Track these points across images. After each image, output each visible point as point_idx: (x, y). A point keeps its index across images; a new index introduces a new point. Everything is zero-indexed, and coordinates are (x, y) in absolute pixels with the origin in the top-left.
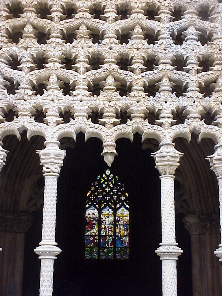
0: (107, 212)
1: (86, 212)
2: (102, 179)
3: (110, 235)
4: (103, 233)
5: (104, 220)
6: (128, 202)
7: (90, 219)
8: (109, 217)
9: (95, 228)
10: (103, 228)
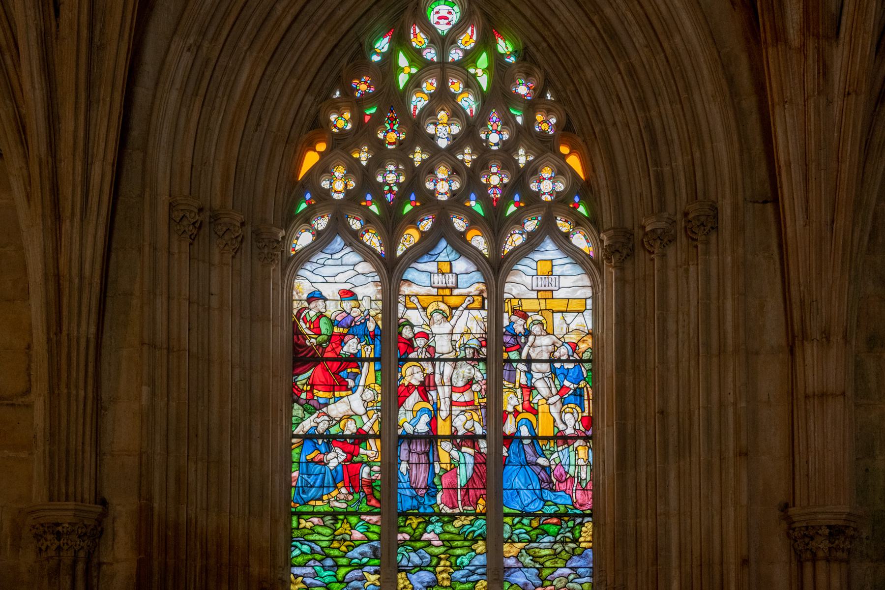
0: (438, 280)
2: (402, 60)
4: (412, 417)
5: (417, 330)
6: (582, 209)
7: (324, 326)
9: (360, 389)
10: (410, 388)
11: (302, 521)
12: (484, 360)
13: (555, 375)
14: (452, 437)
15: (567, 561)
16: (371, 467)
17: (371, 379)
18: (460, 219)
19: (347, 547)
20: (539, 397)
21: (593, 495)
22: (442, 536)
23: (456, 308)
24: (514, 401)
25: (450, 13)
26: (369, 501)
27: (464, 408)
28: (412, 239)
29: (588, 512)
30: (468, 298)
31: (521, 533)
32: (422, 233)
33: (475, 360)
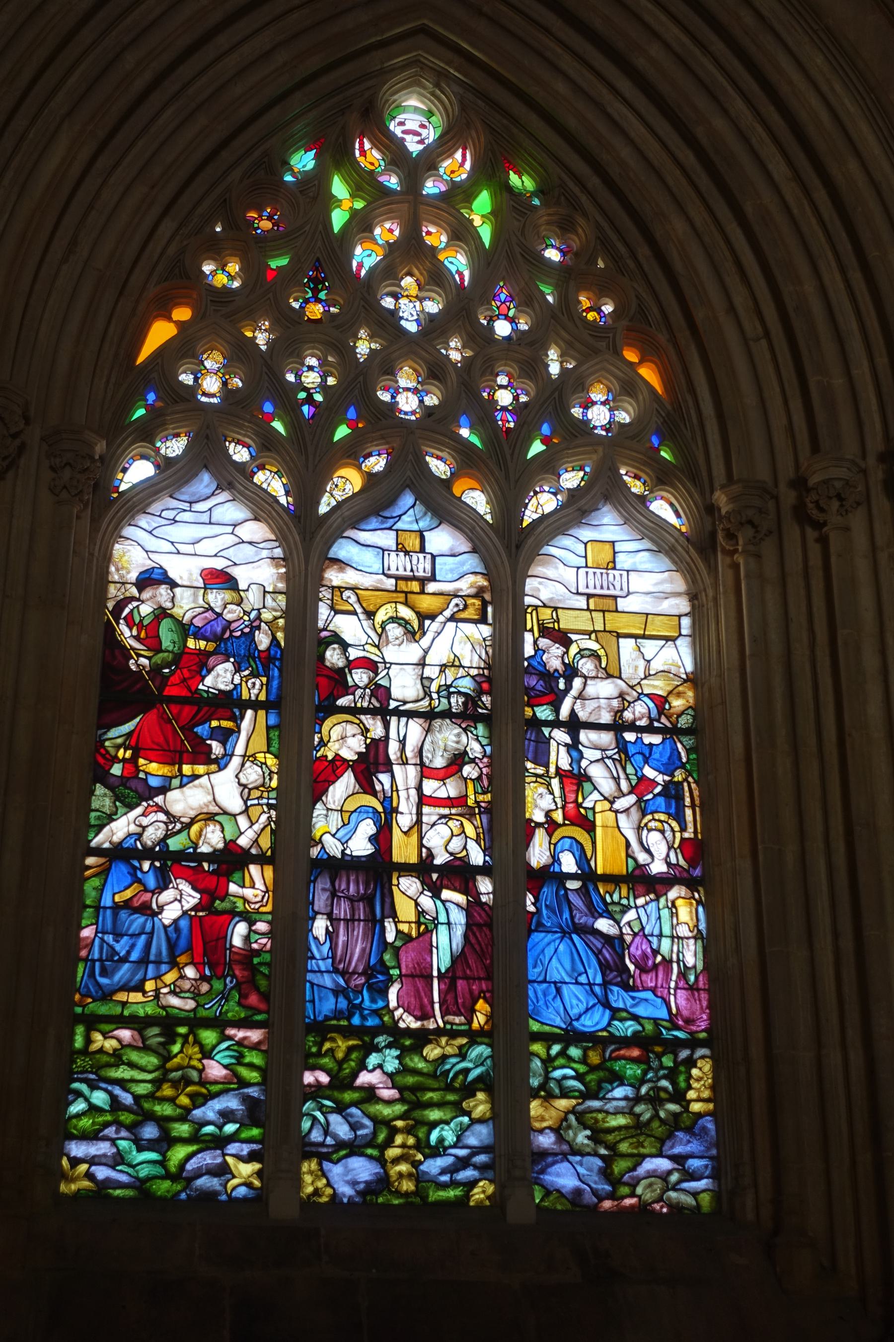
0: (398, 563)
2: (339, 188)
3: (441, 859)
4: (340, 826)
5: (353, 654)
7: (167, 636)
8: (432, 627)
9: (236, 761)
10: (338, 766)
11: (97, 1037)
12: (487, 720)
14: (423, 868)
15: (662, 1141)
16: (251, 923)
17: (259, 741)
18: (439, 458)
19: (191, 1096)
20: (595, 796)
21: (709, 1001)
22: (398, 1078)
23: (433, 617)
24: (546, 802)
25: (423, 126)
26: (243, 996)
27: (446, 811)
28: (348, 486)
29: (703, 1035)
30: (455, 601)
31: (565, 1077)
32: (371, 478)
33: (468, 716)
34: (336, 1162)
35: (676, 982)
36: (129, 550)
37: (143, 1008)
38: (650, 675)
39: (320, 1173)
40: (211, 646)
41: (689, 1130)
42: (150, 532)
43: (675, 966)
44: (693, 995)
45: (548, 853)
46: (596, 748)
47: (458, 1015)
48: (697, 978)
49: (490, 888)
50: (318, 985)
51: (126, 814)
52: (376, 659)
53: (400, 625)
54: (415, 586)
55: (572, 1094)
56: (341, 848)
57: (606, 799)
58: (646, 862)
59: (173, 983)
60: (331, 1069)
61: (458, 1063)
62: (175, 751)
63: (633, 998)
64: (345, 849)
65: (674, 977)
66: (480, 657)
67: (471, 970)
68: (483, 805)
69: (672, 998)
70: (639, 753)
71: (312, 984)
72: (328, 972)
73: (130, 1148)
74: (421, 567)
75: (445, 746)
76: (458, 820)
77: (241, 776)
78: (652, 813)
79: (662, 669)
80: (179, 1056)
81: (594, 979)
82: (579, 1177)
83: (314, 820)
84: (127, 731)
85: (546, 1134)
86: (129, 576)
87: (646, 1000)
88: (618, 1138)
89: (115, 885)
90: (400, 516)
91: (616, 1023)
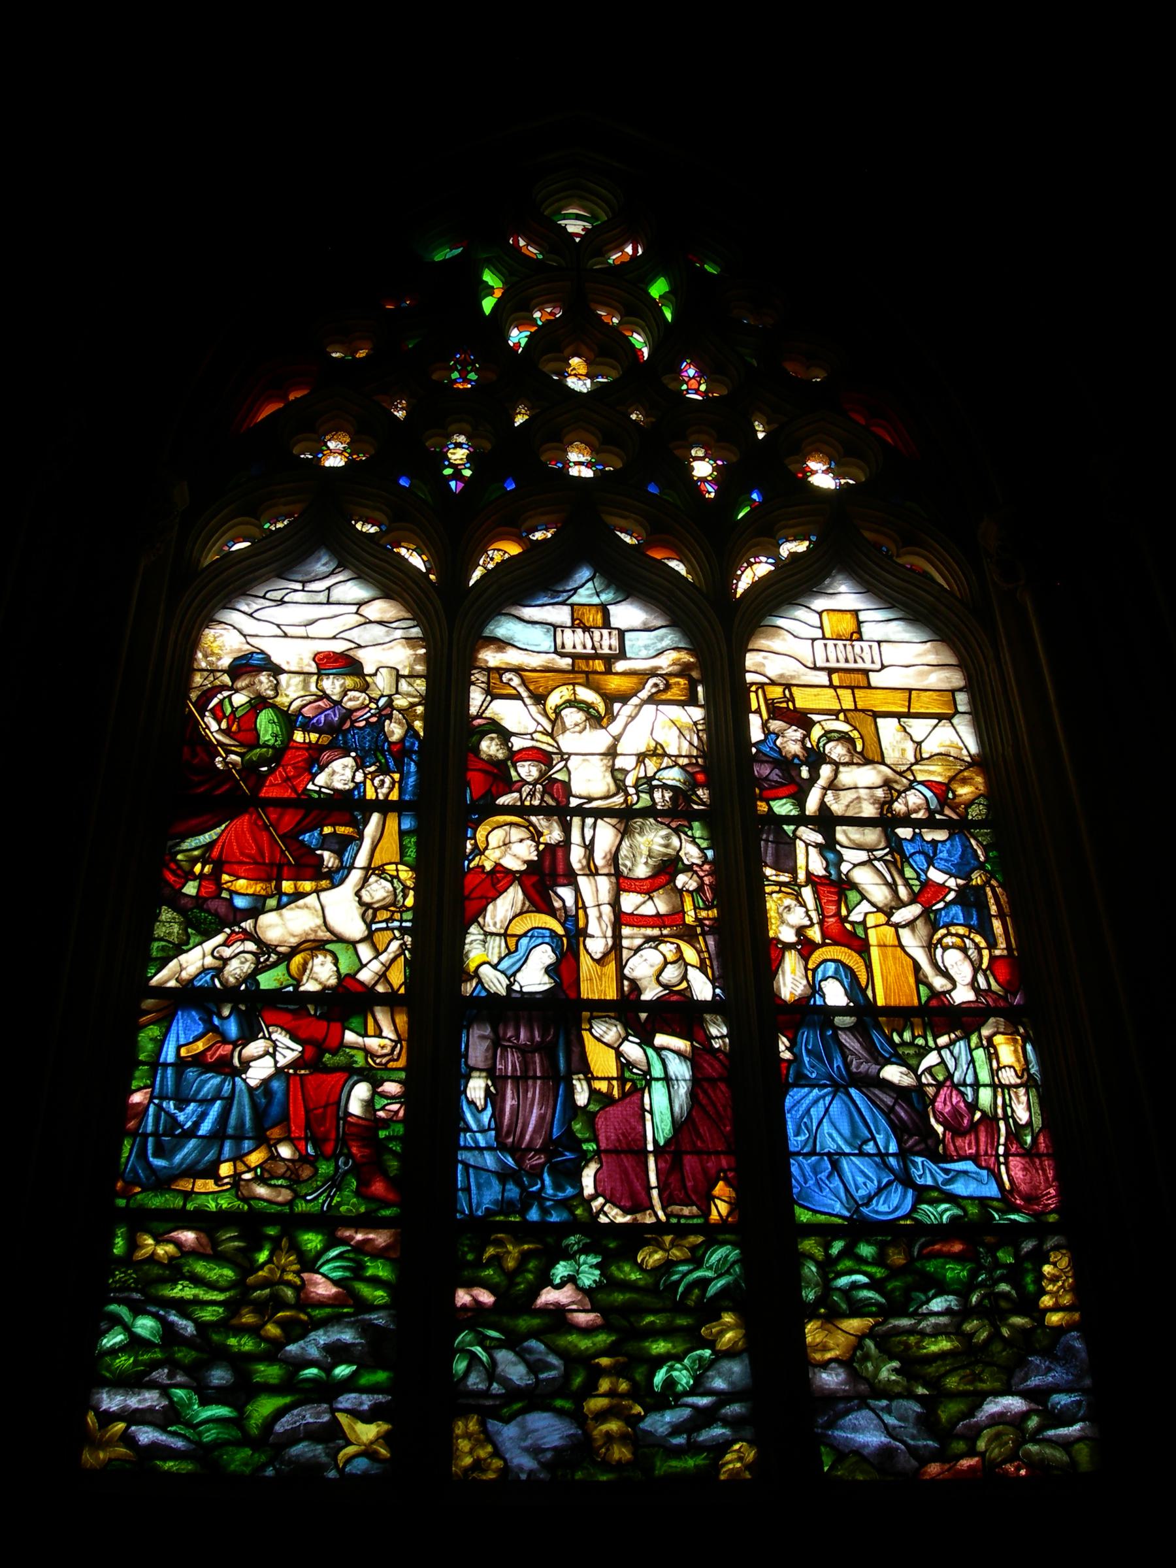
0: (574, 640)
1: (210, 634)
3: (650, 993)
4: (506, 954)
5: (517, 744)
7: (266, 726)
8: (623, 711)
9: (356, 876)
10: (500, 878)
13: (902, 852)
17: (389, 849)
20: (865, 907)
22: (600, 1296)
23: (624, 699)
24: (797, 917)
27: (656, 932)
29: (1052, 1218)
31: (855, 1286)
33: (678, 813)
34: (507, 1421)
35: (1005, 1145)
36: (221, 635)
37: (215, 1200)
38: (923, 759)
39: (482, 1436)
40: (325, 739)
41: (1046, 1352)
42: (251, 615)
43: (1002, 1125)
44: (1034, 1163)
45: (804, 982)
46: (859, 847)
47: (687, 1206)
48: (1034, 1140)
49: (725, 1031)
50: (475, 1167)
51: (200, 944)
52: (550, 749)
53: (580, 709)
54: (599, 665)
55: (866, 1310)
56: (505, 982)
57: (879, 910)
58: (945, 989)
59: (260, 1166)
60: (497, 1285)
61: (690, 1272)
62: (271, 864)
63: (946, 1171)
64: (512, 984)
65: (1002, 1140)
66: (691, 744)
67: (703, 1141)
68: (707, 922)
69: (1003, 1168)
70: (919, 852)
71: (467, 1166)
72: (489, 1148)
73: (190, 1399)
74: (605, 643)
75: (650, 850)
76: (672, 943)
77: (363, 893)
78: (947, 926)
79: (938, 751)
80: (266, 1269)
81: (887, 1147)
82: (888, 1430)
83: (467, 947)
84: (208, 840)
85: (832, 1369)
86: (219, 663)
87: (965, 1173)
88: (942, 1370)
89: (182, 1036)
90: (575, 590)
91: (925, 1207)
